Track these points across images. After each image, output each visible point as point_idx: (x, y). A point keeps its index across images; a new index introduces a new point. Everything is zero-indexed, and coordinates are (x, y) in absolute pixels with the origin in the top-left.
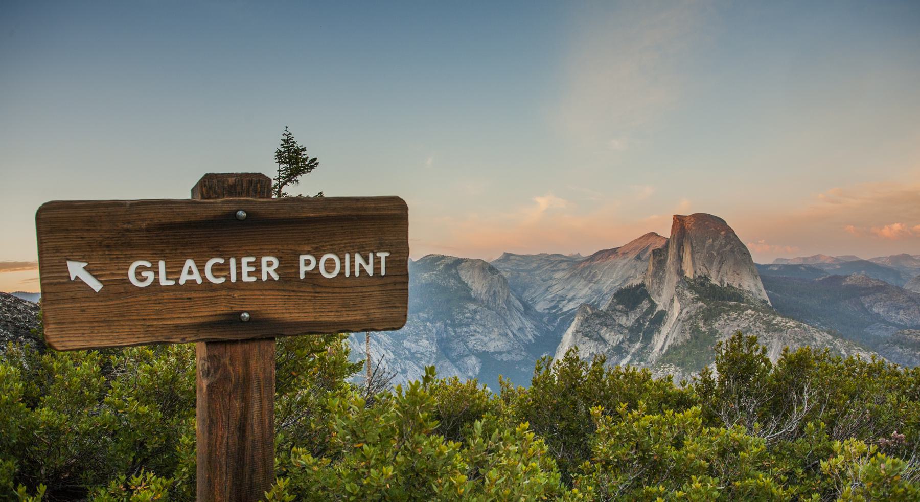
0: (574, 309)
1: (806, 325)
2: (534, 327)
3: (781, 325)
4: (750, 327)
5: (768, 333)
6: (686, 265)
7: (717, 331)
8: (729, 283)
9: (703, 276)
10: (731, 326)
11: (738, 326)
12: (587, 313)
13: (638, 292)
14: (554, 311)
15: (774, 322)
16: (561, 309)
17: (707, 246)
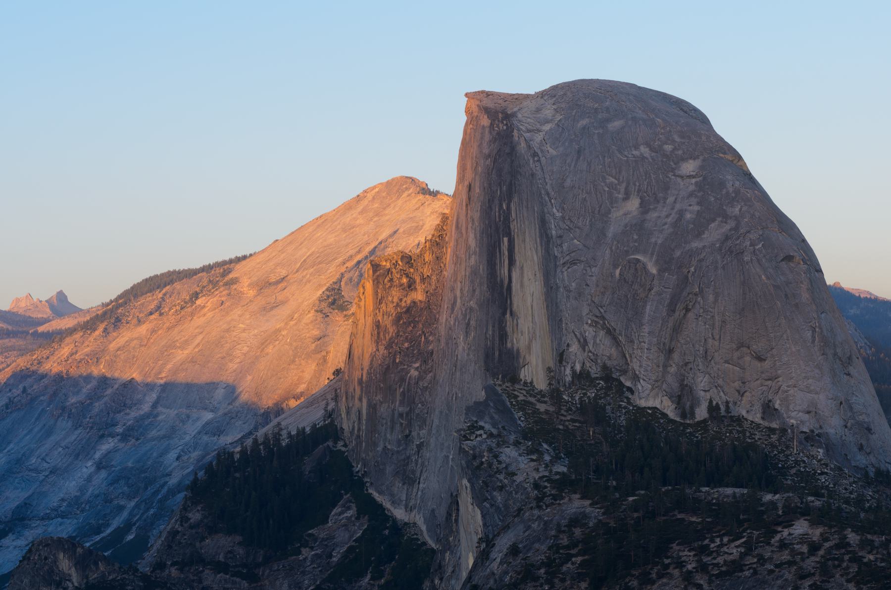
6: (525, 324)
8: (719, 398)
9: (595, 371)
13: (308, 464)
17: (612, 231)
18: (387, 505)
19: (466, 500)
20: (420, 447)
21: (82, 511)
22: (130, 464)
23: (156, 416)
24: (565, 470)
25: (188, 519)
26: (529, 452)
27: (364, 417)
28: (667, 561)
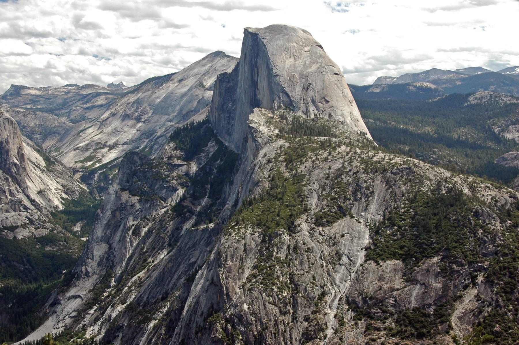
0: (116, 159)
1: (416, 161)
2: (61, 188)
3: (383, 163)
4: (345, 168)
5: (368, 174)
7: (304, 176)
10: (322, 169)
11: (330, 168)
12: (134, 163)
13: (202, 130)
14: (89, 163)
15: (375, 159)
16: (99, 161)
18: (223, 141)
19: (250, 141)
20: (232, 125)
21: (133, 143)
22: (146, 130)
23: (153, 117)
24: (278, 132)
25: (169, 146)
26: (268, 127)
27: (217, 117)
28: (307, 157)
